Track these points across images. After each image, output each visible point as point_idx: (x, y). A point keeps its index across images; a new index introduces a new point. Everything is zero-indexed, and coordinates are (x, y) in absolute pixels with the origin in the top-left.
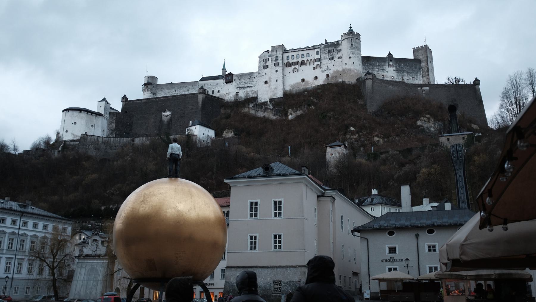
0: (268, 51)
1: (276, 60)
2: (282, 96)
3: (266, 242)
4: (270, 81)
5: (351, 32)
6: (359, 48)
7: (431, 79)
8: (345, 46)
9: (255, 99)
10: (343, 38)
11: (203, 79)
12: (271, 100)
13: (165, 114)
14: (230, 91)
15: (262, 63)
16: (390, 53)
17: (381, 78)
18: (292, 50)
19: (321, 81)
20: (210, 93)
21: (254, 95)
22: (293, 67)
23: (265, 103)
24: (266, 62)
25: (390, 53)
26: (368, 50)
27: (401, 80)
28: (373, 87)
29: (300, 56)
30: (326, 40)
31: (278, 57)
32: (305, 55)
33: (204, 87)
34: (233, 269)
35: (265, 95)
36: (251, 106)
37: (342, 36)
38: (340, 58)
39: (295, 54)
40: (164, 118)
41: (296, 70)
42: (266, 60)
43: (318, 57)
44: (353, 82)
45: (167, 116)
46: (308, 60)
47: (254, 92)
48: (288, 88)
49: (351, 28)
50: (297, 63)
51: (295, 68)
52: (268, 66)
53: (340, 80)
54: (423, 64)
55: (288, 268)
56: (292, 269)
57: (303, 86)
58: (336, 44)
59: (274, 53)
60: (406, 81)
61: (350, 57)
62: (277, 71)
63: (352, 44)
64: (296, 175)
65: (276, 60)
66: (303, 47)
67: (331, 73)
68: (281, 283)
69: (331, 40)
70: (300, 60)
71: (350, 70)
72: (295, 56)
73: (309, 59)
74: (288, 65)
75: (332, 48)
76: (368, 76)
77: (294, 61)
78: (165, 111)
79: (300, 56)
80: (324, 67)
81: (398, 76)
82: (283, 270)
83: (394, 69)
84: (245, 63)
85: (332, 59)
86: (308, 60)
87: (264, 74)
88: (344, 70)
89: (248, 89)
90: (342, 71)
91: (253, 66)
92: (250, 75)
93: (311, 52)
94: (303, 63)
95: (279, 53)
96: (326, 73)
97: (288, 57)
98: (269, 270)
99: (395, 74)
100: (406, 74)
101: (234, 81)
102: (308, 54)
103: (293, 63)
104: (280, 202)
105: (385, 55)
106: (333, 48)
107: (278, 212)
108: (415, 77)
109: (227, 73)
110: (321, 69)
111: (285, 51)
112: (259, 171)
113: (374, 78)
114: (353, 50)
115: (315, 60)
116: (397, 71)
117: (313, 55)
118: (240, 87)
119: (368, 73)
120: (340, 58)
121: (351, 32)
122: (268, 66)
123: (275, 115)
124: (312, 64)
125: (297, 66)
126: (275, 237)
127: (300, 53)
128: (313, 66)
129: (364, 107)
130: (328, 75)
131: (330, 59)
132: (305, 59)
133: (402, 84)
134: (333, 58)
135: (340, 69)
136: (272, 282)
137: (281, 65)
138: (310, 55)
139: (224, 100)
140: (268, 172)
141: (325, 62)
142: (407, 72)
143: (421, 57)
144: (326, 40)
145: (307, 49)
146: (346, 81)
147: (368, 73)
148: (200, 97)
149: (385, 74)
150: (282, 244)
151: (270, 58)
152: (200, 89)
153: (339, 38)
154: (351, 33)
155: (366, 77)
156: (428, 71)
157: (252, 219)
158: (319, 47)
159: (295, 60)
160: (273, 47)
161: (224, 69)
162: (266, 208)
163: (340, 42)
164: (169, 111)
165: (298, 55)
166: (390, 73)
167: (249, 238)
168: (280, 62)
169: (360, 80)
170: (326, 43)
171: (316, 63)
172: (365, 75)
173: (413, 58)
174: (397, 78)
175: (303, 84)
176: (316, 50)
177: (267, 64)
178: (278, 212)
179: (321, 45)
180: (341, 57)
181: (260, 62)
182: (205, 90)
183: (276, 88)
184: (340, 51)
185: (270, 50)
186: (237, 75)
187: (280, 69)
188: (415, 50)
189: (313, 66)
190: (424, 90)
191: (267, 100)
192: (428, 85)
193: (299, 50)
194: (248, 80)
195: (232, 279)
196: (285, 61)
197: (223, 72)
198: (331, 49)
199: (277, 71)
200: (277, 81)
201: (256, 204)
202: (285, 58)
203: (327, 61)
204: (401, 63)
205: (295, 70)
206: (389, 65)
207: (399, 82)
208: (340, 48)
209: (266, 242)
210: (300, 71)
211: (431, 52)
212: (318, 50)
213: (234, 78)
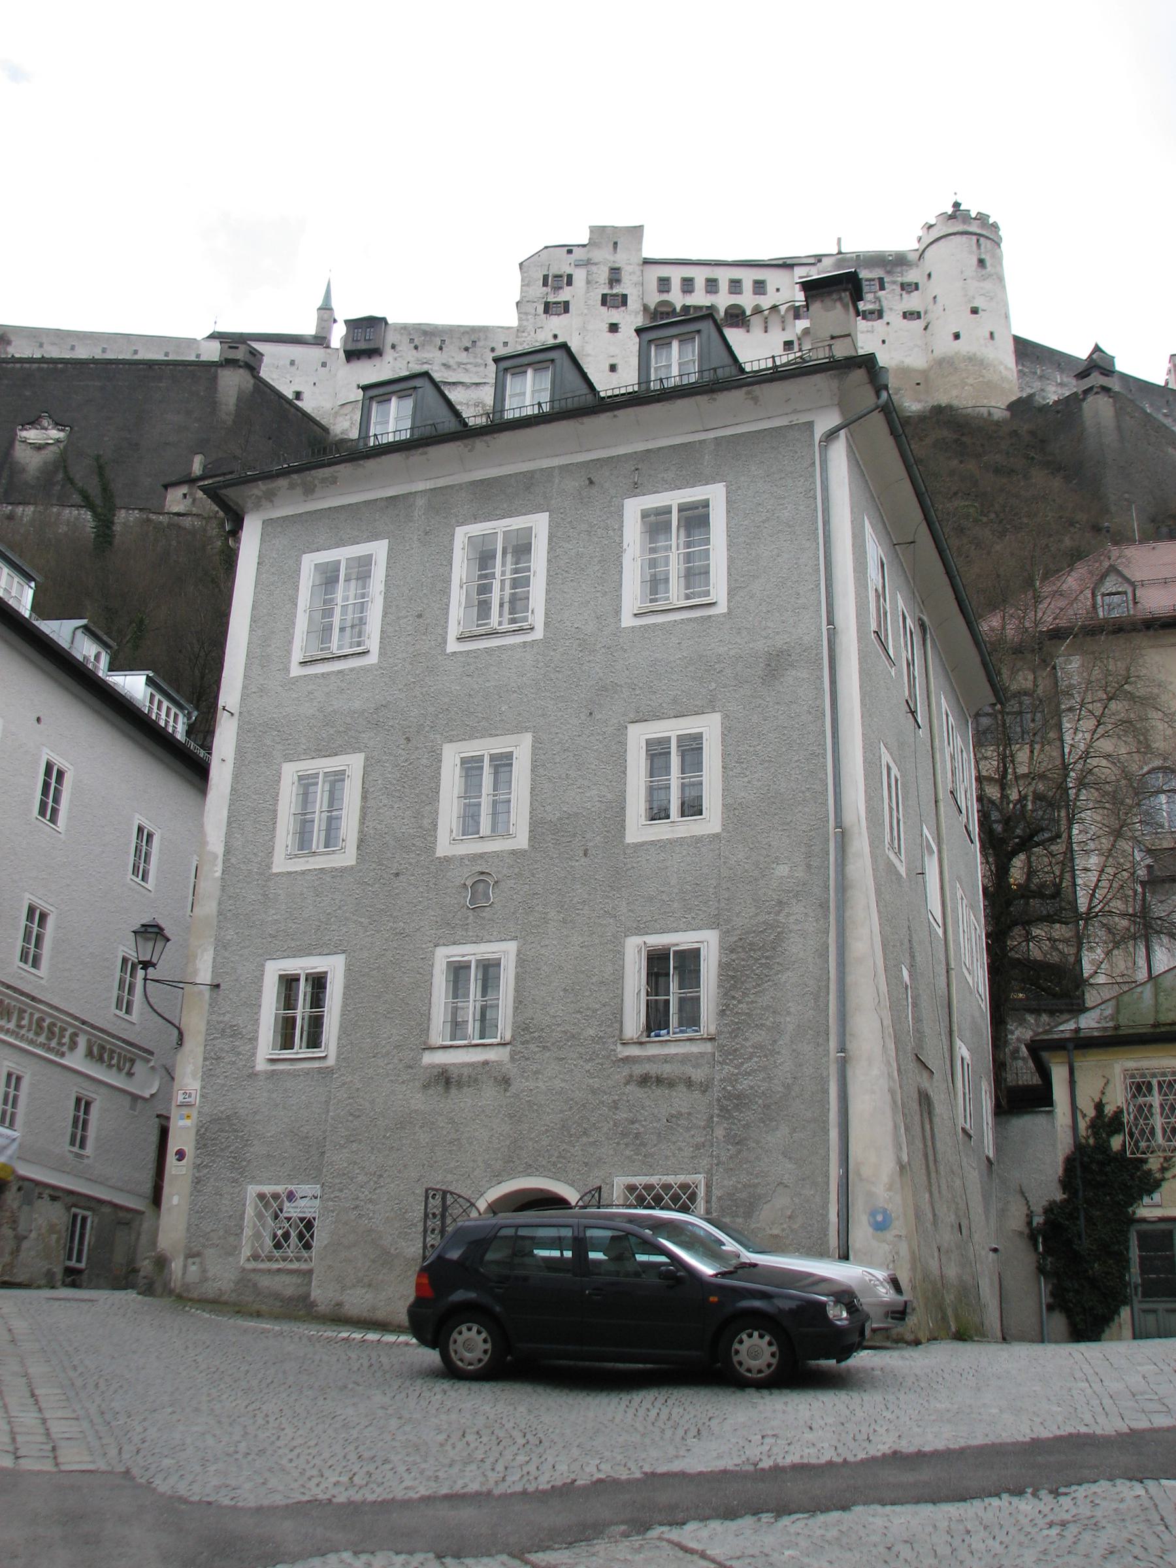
10: (935, 233)
13: (32, 435)
15: (538, 291)
28: (1119, 428)
29: (724, 286)
30: (839, 240)
32: (748, 286)
38: (909, 315)
40: (21, 454)
44: (999, 414)
45: (39, 448)
49: (957, 205)
59: (603, 255)
62: (614, 328)
63: (981, 262)
72: (700, 284)
73: (766, 302)
77: (691, 300)
78: (33, 423)
79: (724, 286)
88: (945, 364)
90: (925, 373)
93: (773, 279)
101: (389, 355)
102: (759, 287)
103: (686, 308)
105: (1082, 352)
114: (987, 285)
120: (909, 315)
132: (747, 300)
138: (770, 288)
139: (326, 430)
144: (839, 240)
148: (232, 383)
151: (580, 276)
159: (700, 298)
161: (326, 308)
164: (57, 424)
165: (712, 285)
170: (840, 253)
177: (565, 295)
181: (526, 284)
184: (909, 288)
186: (404, 328)
194: (463, 357)
197: (321, 320)
202: (653, 285)
213: (391, 338)
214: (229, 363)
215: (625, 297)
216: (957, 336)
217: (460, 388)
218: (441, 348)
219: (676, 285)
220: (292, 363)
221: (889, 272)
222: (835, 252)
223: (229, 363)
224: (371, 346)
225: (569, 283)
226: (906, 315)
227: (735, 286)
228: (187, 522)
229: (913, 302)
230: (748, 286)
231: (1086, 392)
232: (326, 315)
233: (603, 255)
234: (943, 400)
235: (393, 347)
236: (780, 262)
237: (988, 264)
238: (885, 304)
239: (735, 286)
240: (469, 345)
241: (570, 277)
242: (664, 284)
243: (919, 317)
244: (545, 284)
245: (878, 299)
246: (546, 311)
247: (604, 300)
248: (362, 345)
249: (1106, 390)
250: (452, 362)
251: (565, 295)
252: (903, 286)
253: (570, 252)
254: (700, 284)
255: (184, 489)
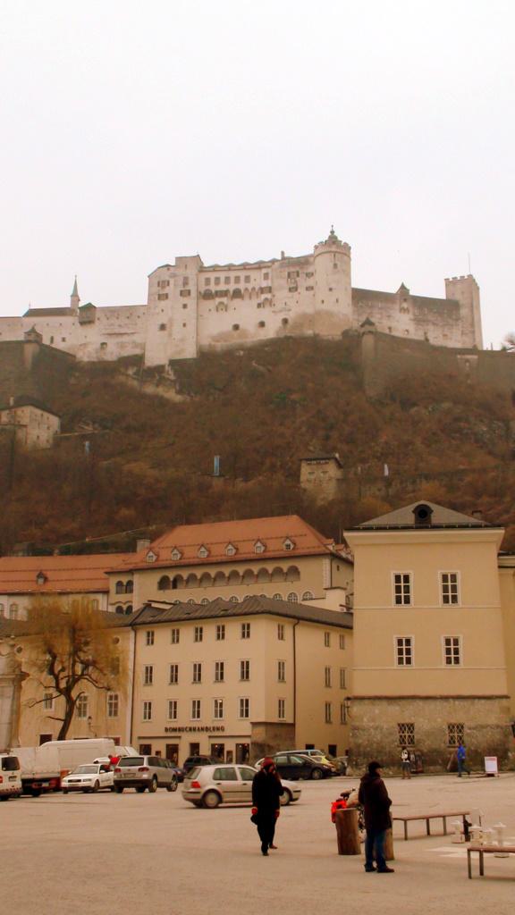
0: (167, 266)
1: (186, 283)
2: (195, 356)
3: (428, 651)
4: (171, 326)
5: (333, 240)
6: (347, 273)
7: (477, 340)
8: (322, 266)
9: (137, 360)
10: (318, 252)
11: (33, 313)
12: (173, 363)
14: (88, 340)
15: (156, 289)
16: (403, 287)
17: (387, 331)
18: (215, 268)
19: (271, 332)
20: (46, 341)
21: (138, 351)
22: (218, 300)
23: (160, 369)
24: (163, 287)
25: (403, 287)
26: (362, 278)
27: (422, 338)
29: (232, 280)
30: (283, 253)
31: (186, 281)
32: (242, 279)
33: (38, 330)
34: (366, 702)
35: (158, 354)
36: (131, 372)
37: (316, 247)
38: (310, 288)
39: (222, 276)
41: (222, 307)
42: (163, 284)
43: (264, 284)
46: (246, 289)
47: (136, 345)
48: (205, 342)
49: (332, 232)
50: (224, 294)
51: (221, 303)
52: (167, 296)
53: (310, 332)
54: (464, 312)
55: (476, 701)
56: (483, 701)
57: (236, 340)
58: (303, 262)
59: (181, 272)
60: (432, 341)
61: (331, 289)
62: (185, 306)
63: (335, 266)
64: (486, 526)
65: (186, 283)
66: (237, 262)
67: (291, 316)
68: (462, 727)
69: (295, 252)
70: (232, 287)
71: (329, 314)
72: (222, 280)
73: (250, 286)
74: (208, 296)
75: (296, 268)
76: (368, 328)
79: (232, 280)
80: (279, 306)
81: (416, 330)
82: (466, 703)
83: (411, 316)
84: (121, 284)
85: (293, 289)
86: (246, 289)
87: (158, 310)
88: (318, 313)
89: (125, 339)
91: (136, 294)
92: (130, 312)
94: (237, 294)
95: (191, 272)
96: (283, 316)
97: (208, 281)
98: (438, 702)
99: (411, 327)
100: (431, 327)
101: (97, 322)
102: (247, 279)
103: (216, 292)
104: (454, 577)
106: (297, 269)
107: (450, 596)
108: (448, 334)
109: (81, 304)
110: (273, 309)
111: (202, 269)
112: (406, 515)
113: (375, 334)
115: (262, 290)
116: (418, 321)
117: (258, 280)
118: (110, 334)
119: (368, 322)
120: (310, 288)
121: (333, 240)
122: (167, 296)
123: (179, 392)
124: (254, 297)
125: (225, 300)
126: (448, 642)
127: (232, 275)
128: (255, 302)
129: (359, 385)
130: (285, 321)
131: (290, 290)
132: (242, 286)
133: (424, 344)
134: (296, 289)
135: (309, 310)
136: (445, 727)
137: (194, 294)
138: (252, 279)
139: (75, 357)
140: (423, 518)
141: (282, 295)
142: (434, 324)
143: (458, 297)
144: (283, 253)
145: (245, 267)
146: (322, 333)
147: (368, 322)
148: (30, 350)
149: (393, 325)
150: (461, 656)
151: (172, 282)
152: (28, 334)
153: (309, 251)
154: (334, 243)
155: (362, 330)
156: (472, 325)
157: (399, 606)
158: (269, 264)
159: (222, 287)
160: (179, 259)
161: (75, 296)
162: (426, 589)
163: (312, 259)
165: (227, 280)
166: (402, 325)
167: (395, 643)
168: (192, 287)
169: (351, 333)
170: (284, 258)
171: (263, 296)
172: (362, 326)
173: (444, 297)
174: (415, 334)
175: (236, 333)
176: (264, 271)
177: (167, 290)
178: (450, 596)
179: (273, 261)
180: (312, 288)
181: (150, 286)
182: (39, 336)
183: (182, 340)
185: (173, 263)
186: (103, 309)
187: (191, 302)
188: (450, 283)
189: (255, 302)
190: (467, 361)
191: (164, 361)
192: (474, 350)
193: (230, 267)
194: (127, 321)
195: (365, 720)
196: (203, 289)
197: (72, 301)
198: (292, 269)
199: (185, 306)
200: (184, 325)
201: (407, 578)
203: (285, 292)
204: (423, 304)
205: (223, 307)
206: (403, 310)
207: (418, 343)
208: (311, 269)
209: (428, 651)
210: (231, 311)
211: (478, 288)
212: (269, 270)
213: (98, 314)
214: (28, 342)
215: (189, 292)
216: (323, 302)
217: (125, 336)
218: (118, 318)
219: (212, 281)
220: (61, 324)
221: (302, 268)
222: (280, 258)
223: (28, 342)
224: (90, 319)
225: (168, 285)
226: (307, 289)
227: (237, 279)
228: (7, 427)
229: (310, 282)
230: (242, 279)
231: (364, 333)
232: (76, 298)
233: (181, 272)
234: (317, 332)
235: (98, 319)
236: (257, 266)
237: (339, 266)
238: (299, 283)
239: (237, 279)
240: (128, 315)
241: (168, 282)
242: (208, 281)
243: (312, 288)
244: (159, 285)
245: (296, 282)
246: (159, 299)
247: (182, 293)
248: (86, 320)
249: (370, 332)
250: (122, 324)
251: (167, 290)
252: (307, 275)
253: (168, 269)
254: (222, 280)
255: (7, 412)
